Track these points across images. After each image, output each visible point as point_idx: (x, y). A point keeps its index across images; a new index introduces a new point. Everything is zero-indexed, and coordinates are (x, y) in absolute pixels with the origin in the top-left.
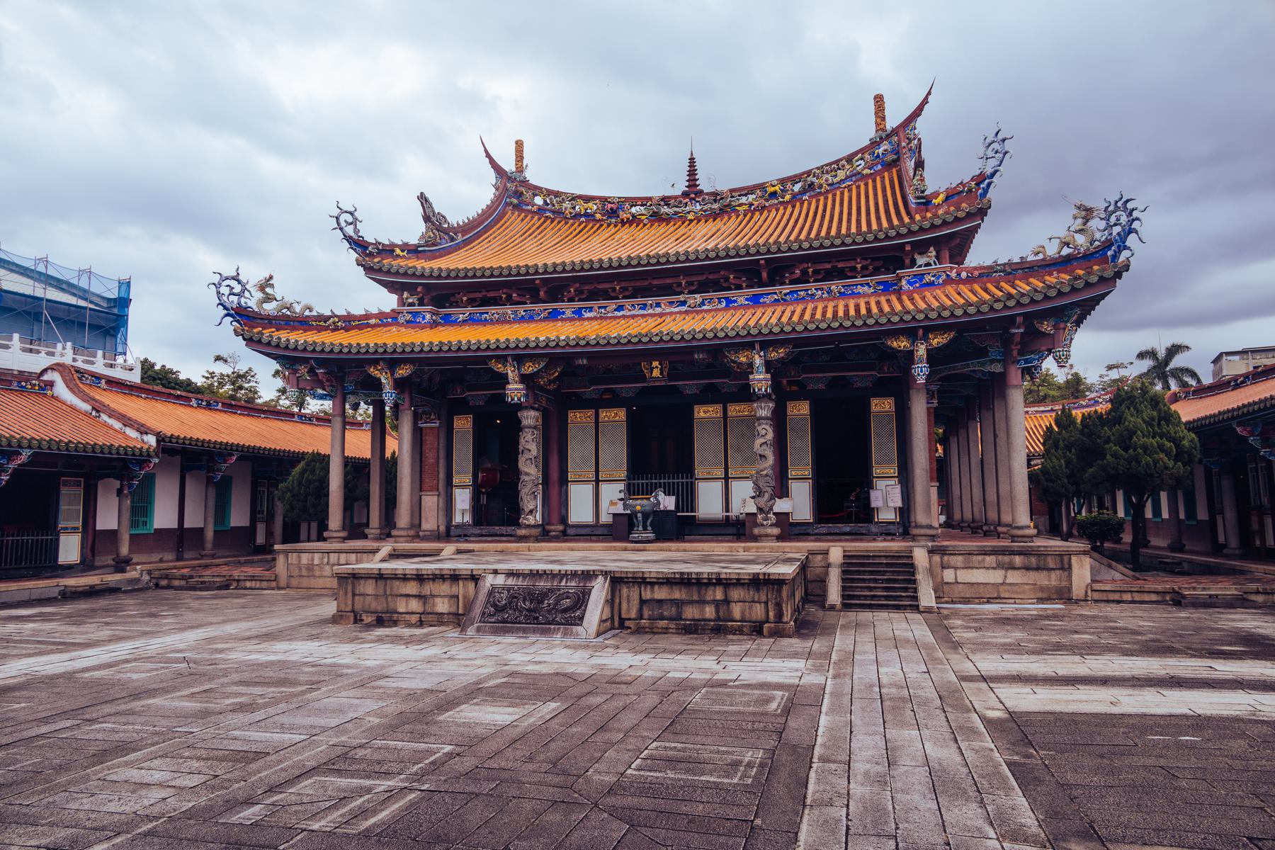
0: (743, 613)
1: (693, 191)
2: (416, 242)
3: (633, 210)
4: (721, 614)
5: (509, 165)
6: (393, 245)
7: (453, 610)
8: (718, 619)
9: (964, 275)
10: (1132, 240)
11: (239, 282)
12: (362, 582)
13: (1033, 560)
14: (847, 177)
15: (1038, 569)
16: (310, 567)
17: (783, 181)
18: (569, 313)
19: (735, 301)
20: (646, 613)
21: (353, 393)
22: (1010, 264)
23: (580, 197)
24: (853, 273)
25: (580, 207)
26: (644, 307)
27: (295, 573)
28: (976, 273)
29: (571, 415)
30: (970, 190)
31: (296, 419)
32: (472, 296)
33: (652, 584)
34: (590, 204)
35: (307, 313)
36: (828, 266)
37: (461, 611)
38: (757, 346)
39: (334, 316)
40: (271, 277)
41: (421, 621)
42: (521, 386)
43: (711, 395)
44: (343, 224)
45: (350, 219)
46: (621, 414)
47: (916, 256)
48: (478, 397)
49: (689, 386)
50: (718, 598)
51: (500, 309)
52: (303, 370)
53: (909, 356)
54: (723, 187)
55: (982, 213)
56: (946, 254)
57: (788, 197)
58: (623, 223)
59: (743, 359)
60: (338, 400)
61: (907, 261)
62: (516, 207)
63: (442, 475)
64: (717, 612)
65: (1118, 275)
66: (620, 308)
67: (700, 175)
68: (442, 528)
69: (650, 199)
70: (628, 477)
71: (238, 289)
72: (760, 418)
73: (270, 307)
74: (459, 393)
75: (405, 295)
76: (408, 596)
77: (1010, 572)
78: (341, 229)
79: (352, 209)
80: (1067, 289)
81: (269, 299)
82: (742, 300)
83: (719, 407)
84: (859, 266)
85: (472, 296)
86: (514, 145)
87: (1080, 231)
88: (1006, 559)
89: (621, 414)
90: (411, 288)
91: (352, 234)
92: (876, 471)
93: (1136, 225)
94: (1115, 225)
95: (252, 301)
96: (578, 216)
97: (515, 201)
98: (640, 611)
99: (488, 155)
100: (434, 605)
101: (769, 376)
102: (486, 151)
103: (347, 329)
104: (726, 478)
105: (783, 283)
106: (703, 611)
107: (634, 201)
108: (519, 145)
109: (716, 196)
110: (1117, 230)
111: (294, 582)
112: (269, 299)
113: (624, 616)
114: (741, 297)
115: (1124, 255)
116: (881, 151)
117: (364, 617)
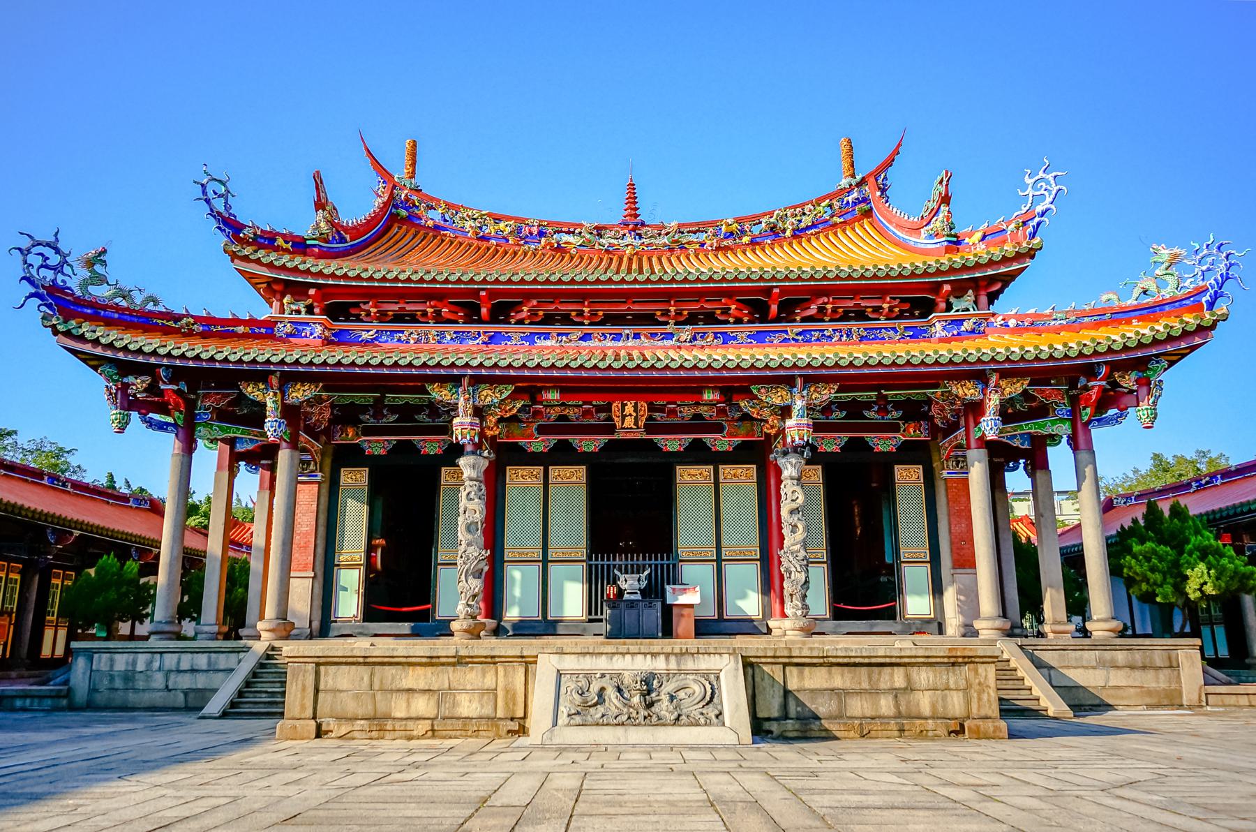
0: (933, 706)
4: (903, 709)
7: (488, 711)
8: (899, 715)
11: (58, 251)
12: (333, 669)
14: (814, 226)
16: (129, 676)
17: (739, 221)
21: (206, 425)
26: (617, 337)
29: (510, 471)
31: (45, 482)
34: (502, 225)
35: (150, 307)
36: (851, 304)
37: (500, 714)
40: (104, 252)
41: (433, 730)
43: (698, 454)
44: (211, 195)
47: (952, 300)
48: (377, 446)
49: (672, 443)
50: (897, 685)
52: (138, 384)
53: (976, 409)
55: (1031, 254)
57: (746, 239)
59: (778, 401)
61: (943, 305)
62: (404, 221)
64: (897, 705)
66: (586, 337)
68: (316, 624)
69: (581, 226)
70: (590, 558)
74: (350, 436)
76: (409, 690)
78: (208, 201)
79: (224, 178)
88: (1108, 655)
89: (577, 475)
91: (222, 209)
92: (905, 554)
95: (74, 281)
97: (404, 213)
100: (455, 705)
101: (811, 422)
103: (205, 335)
104: (719, 561)
105: (794, 321)
106: (876, 704)
107: (560, 228)
112: (102, 280)
113: (760, 715)
116: (850, 199)
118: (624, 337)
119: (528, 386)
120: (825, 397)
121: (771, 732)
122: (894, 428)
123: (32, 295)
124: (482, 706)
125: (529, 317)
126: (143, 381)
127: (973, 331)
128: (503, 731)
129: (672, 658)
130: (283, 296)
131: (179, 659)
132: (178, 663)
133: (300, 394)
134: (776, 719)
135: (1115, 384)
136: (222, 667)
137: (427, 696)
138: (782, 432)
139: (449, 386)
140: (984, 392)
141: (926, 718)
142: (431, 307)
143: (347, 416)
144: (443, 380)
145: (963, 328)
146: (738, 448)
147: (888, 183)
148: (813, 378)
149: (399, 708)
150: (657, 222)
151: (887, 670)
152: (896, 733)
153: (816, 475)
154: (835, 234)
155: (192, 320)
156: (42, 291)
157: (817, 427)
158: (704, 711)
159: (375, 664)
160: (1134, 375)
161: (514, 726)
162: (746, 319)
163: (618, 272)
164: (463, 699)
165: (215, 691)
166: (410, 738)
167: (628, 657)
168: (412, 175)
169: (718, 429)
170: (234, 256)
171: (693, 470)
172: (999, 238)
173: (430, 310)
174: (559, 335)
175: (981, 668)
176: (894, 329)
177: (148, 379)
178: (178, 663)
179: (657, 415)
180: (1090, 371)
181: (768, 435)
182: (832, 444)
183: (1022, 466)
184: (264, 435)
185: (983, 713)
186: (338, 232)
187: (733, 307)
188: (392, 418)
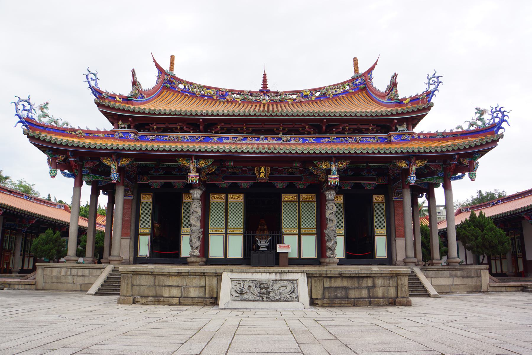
0: (383, 293)
1: (265, 90)
2: (127, 95)
3: (233, 96)
4: (371, 294)
5: (166, 67)
6: (114, 94)
7: (202, 295)
8: (369, 297)
9: (421, 137)
10: (504, 125)
11: (29, 104)
12: (139, 277)
13: (465, 273)
14: (342, 93)
15: (467, 277)
16: (58, 277)
17: (311, 90)
18: (215, 139)
19: (307, 140)
20: (327, 295)
21: (87, 175)
22: (444, 133)
23: (205, 86)
24: (367, 131)
25: (207, 92)
26: (258, 139)
27: (49, 280)
28: (428, 136)
29: (212, 196)
30: (423, 98)
32: (159, 126)
33: (331, 278)
34: (210, 91)
35: (65, 126)
37: (207, 296)
39: (79, 129)
42: (198, 174)
43: (291, 189)
44: (90, 80)
45: (94, 77)
46: (240, 197)
47: (397, 126)
48: (156, 184)
49: (280, 184)
51: (175, 135)
52: (61, 158)
53: (407, 172)
54: (281, 89)
58: (228, 101)
59: (325, 167)
60: (78, 178)
61: (394, 128)
62: (168, 88)
63: (133, 228)
64: (369, 293)
65: (498, 141)
66: (245, 139)
68: (132, 258)
69: (243, 91)
71: (28, 107)
72: (329, 200)
73: (45, 120)
74: (145, 180)
75: (120, 122)
77: (455, 279)
78: (89, 82)
79: (95, 73)
80: (479, 144)
81: (46, 115)
82: (311, 140)
83: (295, 196)
84: (371, 128)
85: (159, 126)
86: (170, 58)
87: (479, 119)
88: (454, 272)
89: (240, 197)
90: (124, 119)
91: (94, 86)
92: (376, 232)
93: (505, 118)
94: (496, 117)
95: (36, 116)
96: (204, 96)
97: (169, 85)
98: (324, 294)
99: (155, 61)
100: (188, 292)
101: (338, 176)
102: (154, 59)
105: (333, 134)
107: (234, 92)
108: (172, 58)
109: (277, 93)
110: (497, 120)
111: (48, 286)
112: (46, 115)
113: (314, 297)
114: (310, 138)
115: (500, 131)
116: (357, 82)
117: (139, 299)
118: (261, 139)
119: (219, 159)
120: (345, 166)
121: (318, 304)
122: (373, 179)
123: (19, 122)
124: (200, 293)
125: (220, 130)
126: (62, 157)
128: (208, 303)
129: (278, 274)
130: (119, 122)
131: (78, 271)
132: (77, 272)
133: (124, 162)
134: (320, 299)
135: (460, 163)
136: (94, 275)
137: (177, 288)
138: (327, 180)
139: (186, 159)
140: (409, 165)
141: (380, 298)
142: (179, 126)
143: (143, 171)
144: (184, 157)
146: (309, 186)
148: (339, 158)
149: (166, 293)
150: (275, 90)
151: (365, 279)
152: (368, 304)
153: (341, 199)
154: (351, 97)
155: (82, 132)
156: (23, 120)
157: (341, 179)
158: (291, 295)
159: (155, 275)
160: (468, 160)
161: (212, 301)
162: (312, 132)
163: (258, 112)
164: (192, 290)
165: (92, 284)
166: (170, 305)
167: (260, 274)
168: (172, 69)
169: (300, 179)
170: (99, 105)
171: (289, 196)
172: (416, 102)
173: (179, 127)
174: (233, 138)
175: (403, 278)
177: (65, 156)
178: (77, 272)
179: (274, 172)
180: (451, 157)
181: (321, 182)
182: (348, 185)
183: (424, 196)
184: (110, 179)
185: (402, 296)
186: (141, 94)
187: (307, 127)
188: (162, 173)
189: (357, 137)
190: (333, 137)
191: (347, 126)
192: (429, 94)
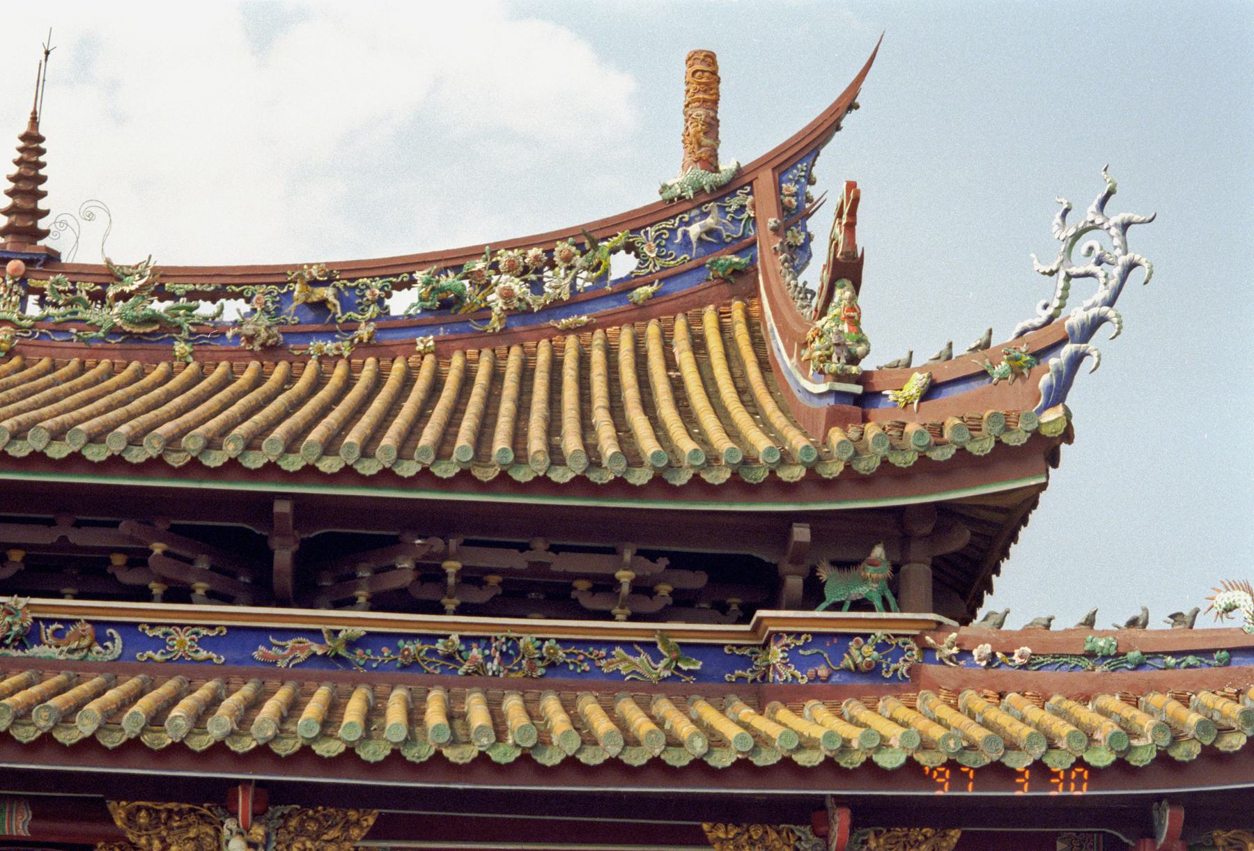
14: (576, 302)
19: (158, 643)
38: (244, 803)
47: (824, 573)
55: (1046, 449)
56: (919, 575)
61: (794, 583)
67: (57, 198)
82: (182, 642)
84: (625, 577)
105: (350, 603)
116: (695, 230)
127: (873, 671)
145: (847, 662)
147: (813, 191)
176: (650, 647)
189: (526, 641)
190: (346, 631)
191: (445, 556)
192: (1055, 352)
